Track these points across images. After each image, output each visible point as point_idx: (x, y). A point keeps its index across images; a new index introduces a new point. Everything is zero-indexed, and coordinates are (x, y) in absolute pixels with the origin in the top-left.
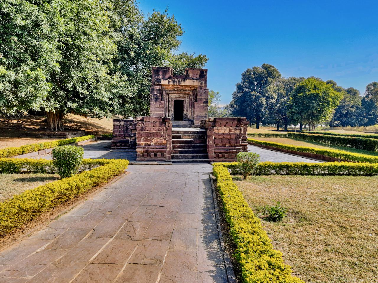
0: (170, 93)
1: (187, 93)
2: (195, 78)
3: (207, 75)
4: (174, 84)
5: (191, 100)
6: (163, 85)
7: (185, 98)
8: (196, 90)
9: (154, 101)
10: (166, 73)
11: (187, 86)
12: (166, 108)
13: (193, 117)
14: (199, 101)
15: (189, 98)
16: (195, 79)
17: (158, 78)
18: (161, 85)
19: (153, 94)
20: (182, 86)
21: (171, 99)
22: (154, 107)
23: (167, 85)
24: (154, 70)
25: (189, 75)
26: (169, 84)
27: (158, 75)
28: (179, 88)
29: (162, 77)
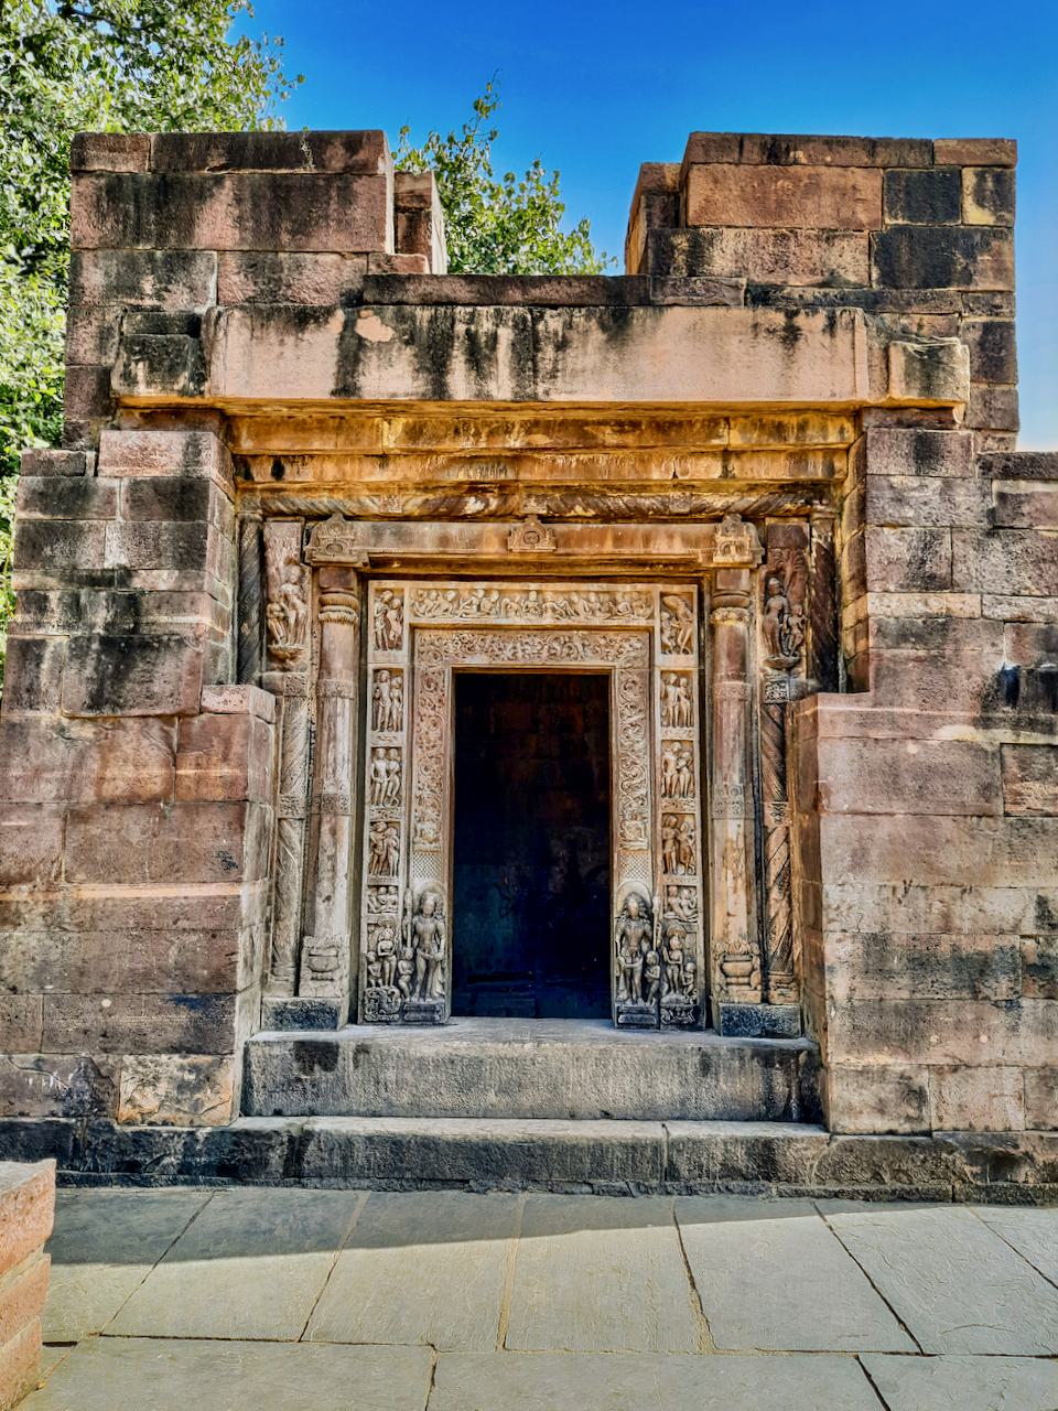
0: (378, 568)
1: (668, 544)
2: (798, 284)
3: (1002, 232)
4: (439, 391)
5: (741, 671)
6: (264, 419)
7: (633, 646)
8: (818, 490)
9: (76, 682)
10: (302, 229)
11: (664, 426)
12: (317, 807)
13: (792, 959)
14: (892, 672)
15: (691, 629)
16: (812, 307)
17: (178, 302)
18: (226, 422)
19: (72, 577)
20: (578, 429)
21: (401, 659)
22: (71, 784)
23: (297, 418)
24: (114, 190)
25: (697, 254)
26: (346, 388)
27: (179, 262)
28: (532, 474)
29: (239, 286)
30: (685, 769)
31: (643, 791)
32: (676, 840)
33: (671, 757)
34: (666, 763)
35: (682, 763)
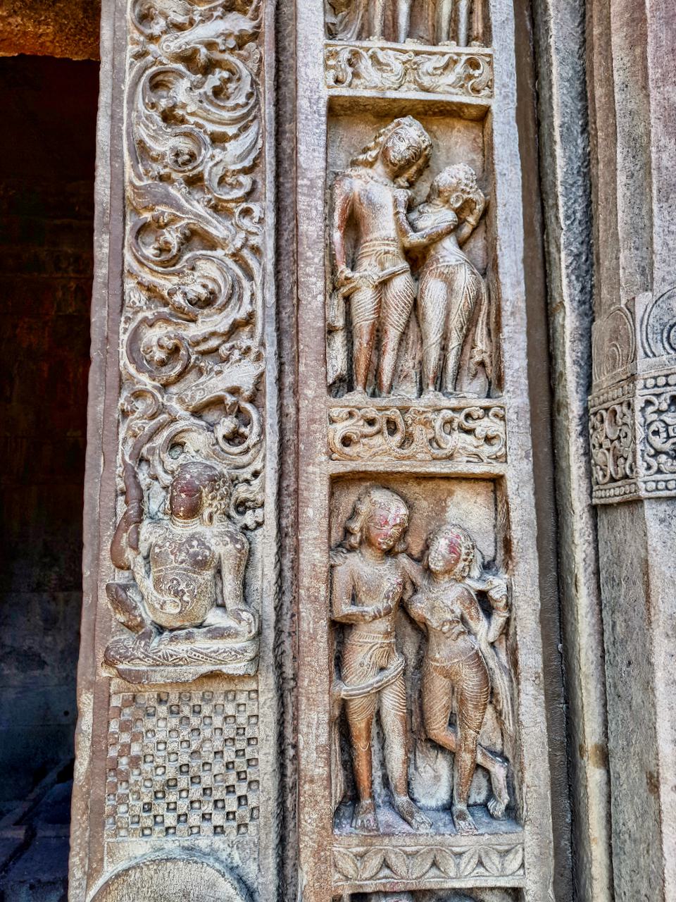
30: (449, 250)
31: (241, 374)
32: (406, 618)
33: (379, 193)
34: (354, 224)
35: (436, 218)
